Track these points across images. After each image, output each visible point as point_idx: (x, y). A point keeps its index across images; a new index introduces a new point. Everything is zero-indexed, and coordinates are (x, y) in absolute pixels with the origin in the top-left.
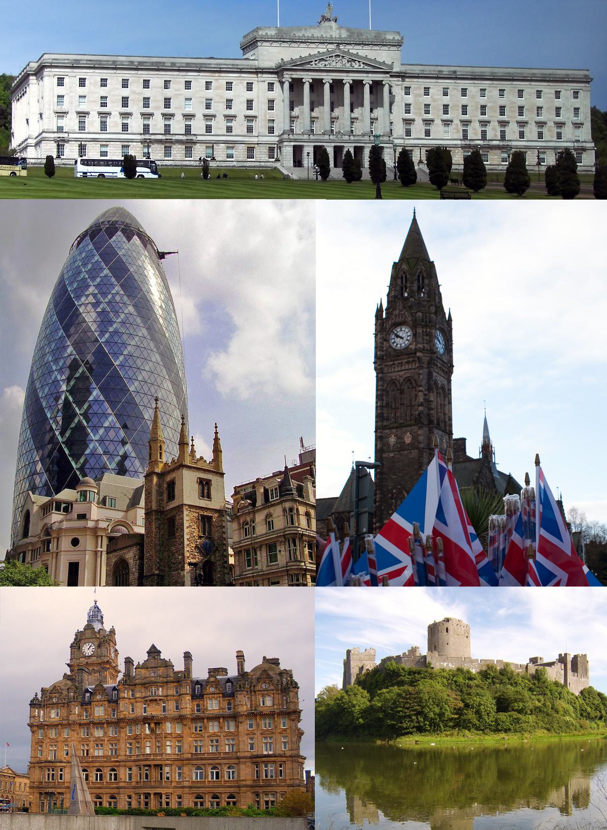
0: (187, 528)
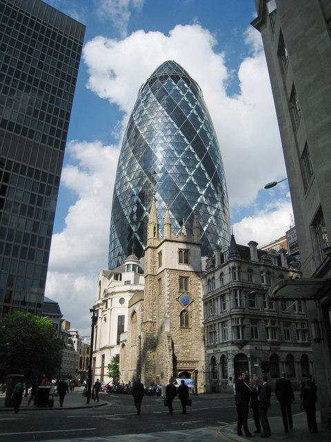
0: (168, 286)
